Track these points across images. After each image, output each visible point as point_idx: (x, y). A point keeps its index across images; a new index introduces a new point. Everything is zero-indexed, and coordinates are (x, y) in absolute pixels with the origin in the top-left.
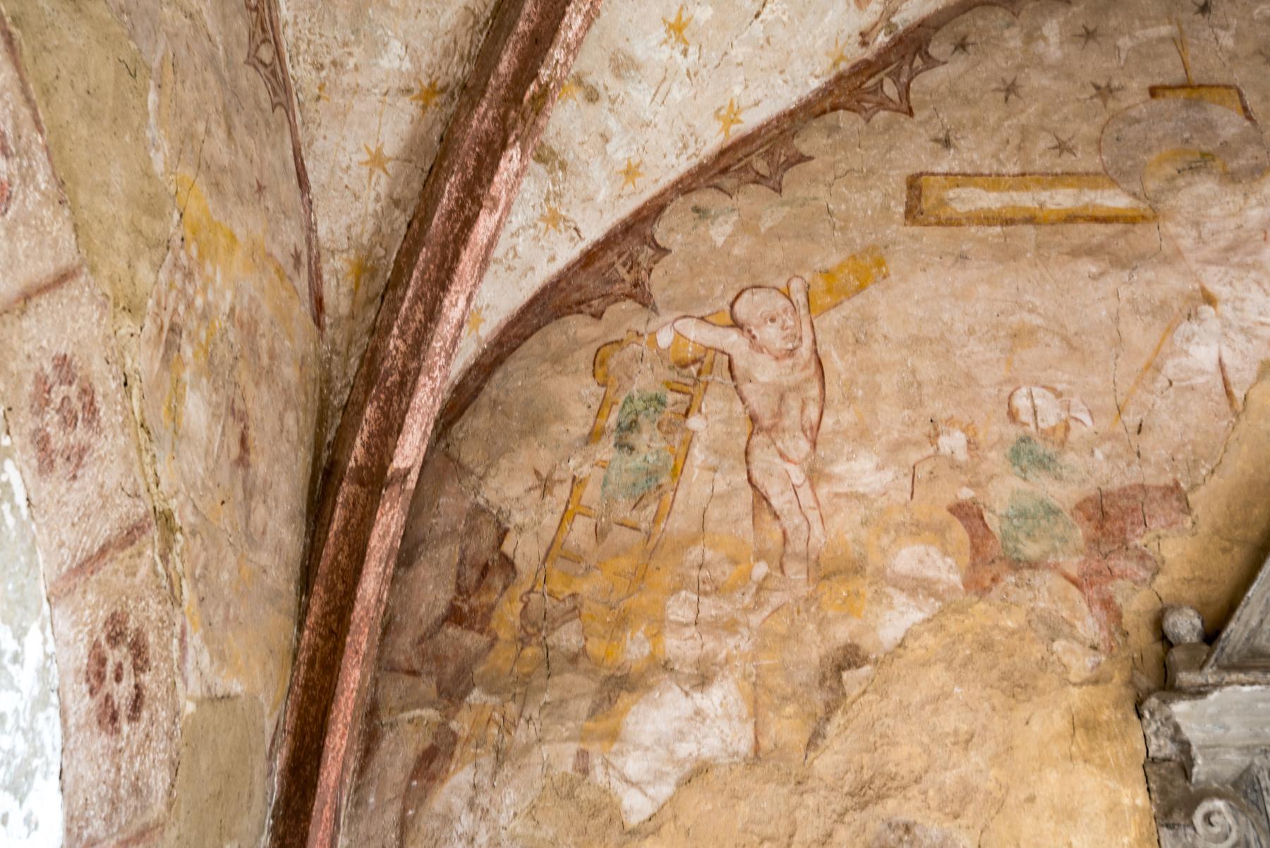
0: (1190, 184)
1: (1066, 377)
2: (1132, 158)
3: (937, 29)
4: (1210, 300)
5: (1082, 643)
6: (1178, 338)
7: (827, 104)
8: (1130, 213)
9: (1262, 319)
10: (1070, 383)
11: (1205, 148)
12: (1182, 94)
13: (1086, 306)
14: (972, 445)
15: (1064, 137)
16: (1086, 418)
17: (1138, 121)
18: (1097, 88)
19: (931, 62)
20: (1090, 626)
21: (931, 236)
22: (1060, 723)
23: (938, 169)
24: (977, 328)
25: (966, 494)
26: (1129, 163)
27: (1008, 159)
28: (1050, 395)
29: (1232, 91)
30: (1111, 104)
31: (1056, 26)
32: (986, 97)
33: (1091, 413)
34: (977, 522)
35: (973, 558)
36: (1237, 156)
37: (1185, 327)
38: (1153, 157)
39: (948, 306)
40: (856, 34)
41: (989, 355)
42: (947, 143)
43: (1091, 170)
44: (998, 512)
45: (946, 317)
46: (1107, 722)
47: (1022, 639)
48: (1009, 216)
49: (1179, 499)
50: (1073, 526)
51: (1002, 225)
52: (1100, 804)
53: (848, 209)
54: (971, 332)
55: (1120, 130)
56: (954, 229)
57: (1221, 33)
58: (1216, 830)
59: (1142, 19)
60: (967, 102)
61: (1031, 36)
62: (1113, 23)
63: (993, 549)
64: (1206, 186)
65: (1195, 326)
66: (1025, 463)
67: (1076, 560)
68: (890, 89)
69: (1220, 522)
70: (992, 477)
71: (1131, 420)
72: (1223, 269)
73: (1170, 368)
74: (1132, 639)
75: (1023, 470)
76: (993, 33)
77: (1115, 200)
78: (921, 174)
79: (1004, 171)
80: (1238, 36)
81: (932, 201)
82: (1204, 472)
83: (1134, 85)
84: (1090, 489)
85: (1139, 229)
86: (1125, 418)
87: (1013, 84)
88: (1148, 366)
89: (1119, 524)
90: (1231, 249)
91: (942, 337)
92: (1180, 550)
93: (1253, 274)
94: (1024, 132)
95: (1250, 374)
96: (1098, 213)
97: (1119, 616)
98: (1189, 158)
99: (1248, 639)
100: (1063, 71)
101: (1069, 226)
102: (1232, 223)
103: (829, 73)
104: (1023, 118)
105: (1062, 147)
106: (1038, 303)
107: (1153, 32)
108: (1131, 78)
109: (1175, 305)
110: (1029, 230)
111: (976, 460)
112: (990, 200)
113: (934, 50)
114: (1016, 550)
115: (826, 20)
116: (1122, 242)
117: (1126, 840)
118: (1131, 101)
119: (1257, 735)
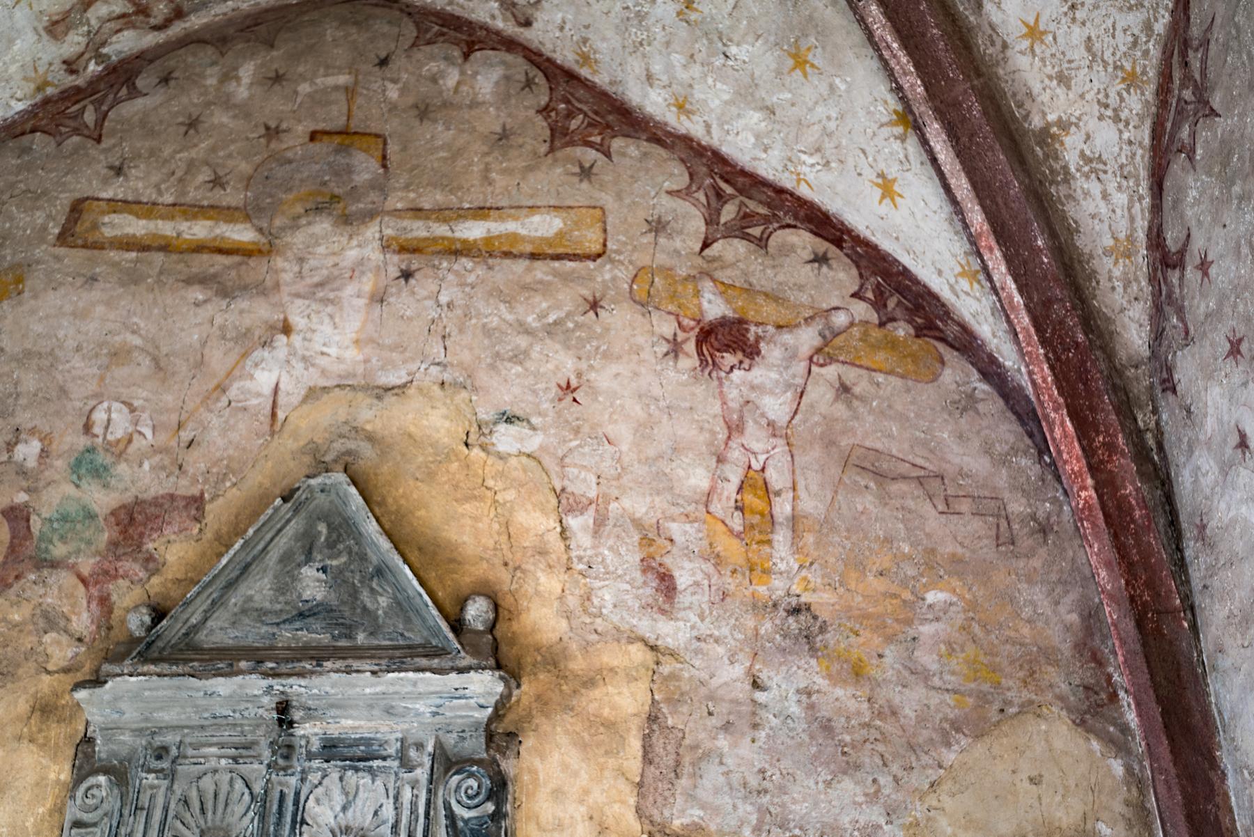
0: (309, 223)
1: (144, 394)
2: (271, 196)
3: (151, 61)
4: (287, 329)
5: (71, 636)
6: (249, 363)
7: (28, 126)
8: (250, 247)
9: (325, 349)
10: (146, 400)
11: (337, 191)
12: (337, 140)
13: (182, 330)
14: (44, 453)
15: (221, 173)
16: (148, 432)
17: (290, 162)
18: (267, 128)
19: (134, 93)
20: (83, 621)
21: (74, 257)
22: (23, 706)
23: (104, 195)
24: (85, 345)
25: (22, 498)
26: (268, 200)
27: (167, 189)
28: (125, 410)
29: (380, 140)
30: (273, 145)
31: (252, 68)
32: (170, 129)
33: (154, 428)
34: (24, 524)
35: (6, 557)
36: (359, 201)
37: (258, 354)
38: (291, 196)
39: (66, 324)
40: (57, 62)
41: (88, 371)
42: (118, 171)
43: (234, 204)
44: (44, 516)
45: (61, 334)
46: (63, 707)
47: (21, 631)
48: (148, 243)
49: (197, 509)
50: (103, 531)
51: (139, 251)
52: (31, 778)
53: (10, 228)
54: (78, 349)
55: (271, 169)
56: (96, 252)
57: (390, 86)
58: (89, 801)
59: (327, 67)
60: (152, 134)
61: (226, 77)
62: (301, 69)
63: (29, 549)
64: (322, 226)
65: (266, 354)
66: (83, 471)
67: (92, 561)
68: (89, 117)
69: (224, 529)
70: (49, 484)
71: (186, 435)
72: (307, 302)
73: (233, 392)
74: (112, 633)
75: (79, 478)
76: (198, 70)
77: (242, 234)
78: (87, 198)
79: (160, 200)
80: (403, 91)
81: (87, 224)
82: (228, 484)
83: (300, 128)
84: (128, 498)
85: (252, 262)
86: (182, 433)
87: (197, 119)
88: (218, 387)
89: (141, 529)
90: (321, 285)
91: (52, 353)
92: (182, 554)
93: (330, 309)
94: (191, 166)
95: (295, 400)
96: (224, 246)
97: (110, 612)
98: (320, 199)
99: (186, 634)
100: (243, 111)
101: (195, 255)
102: (330, 261)
103: (33, 96)
104: (193, 153)
105: (217, 182)
106: (142, 325)
107: (331, 81)
108: (300, 121)
109: (257, 333)
110: (158, 258)
111: (43, 467)
112: (136, 227)
113: (140, 83)
114: (47, 550)
115: (15, 48)
116: (233, 273)
117: (41, 810)
118: (291, 143)
119: (147, 720)
